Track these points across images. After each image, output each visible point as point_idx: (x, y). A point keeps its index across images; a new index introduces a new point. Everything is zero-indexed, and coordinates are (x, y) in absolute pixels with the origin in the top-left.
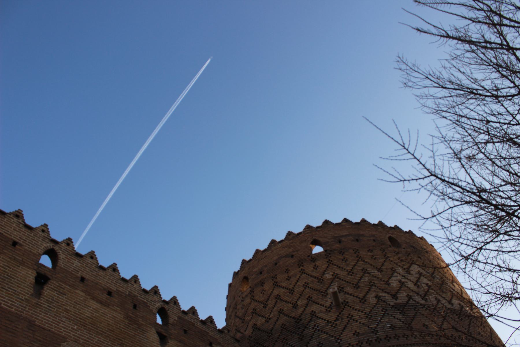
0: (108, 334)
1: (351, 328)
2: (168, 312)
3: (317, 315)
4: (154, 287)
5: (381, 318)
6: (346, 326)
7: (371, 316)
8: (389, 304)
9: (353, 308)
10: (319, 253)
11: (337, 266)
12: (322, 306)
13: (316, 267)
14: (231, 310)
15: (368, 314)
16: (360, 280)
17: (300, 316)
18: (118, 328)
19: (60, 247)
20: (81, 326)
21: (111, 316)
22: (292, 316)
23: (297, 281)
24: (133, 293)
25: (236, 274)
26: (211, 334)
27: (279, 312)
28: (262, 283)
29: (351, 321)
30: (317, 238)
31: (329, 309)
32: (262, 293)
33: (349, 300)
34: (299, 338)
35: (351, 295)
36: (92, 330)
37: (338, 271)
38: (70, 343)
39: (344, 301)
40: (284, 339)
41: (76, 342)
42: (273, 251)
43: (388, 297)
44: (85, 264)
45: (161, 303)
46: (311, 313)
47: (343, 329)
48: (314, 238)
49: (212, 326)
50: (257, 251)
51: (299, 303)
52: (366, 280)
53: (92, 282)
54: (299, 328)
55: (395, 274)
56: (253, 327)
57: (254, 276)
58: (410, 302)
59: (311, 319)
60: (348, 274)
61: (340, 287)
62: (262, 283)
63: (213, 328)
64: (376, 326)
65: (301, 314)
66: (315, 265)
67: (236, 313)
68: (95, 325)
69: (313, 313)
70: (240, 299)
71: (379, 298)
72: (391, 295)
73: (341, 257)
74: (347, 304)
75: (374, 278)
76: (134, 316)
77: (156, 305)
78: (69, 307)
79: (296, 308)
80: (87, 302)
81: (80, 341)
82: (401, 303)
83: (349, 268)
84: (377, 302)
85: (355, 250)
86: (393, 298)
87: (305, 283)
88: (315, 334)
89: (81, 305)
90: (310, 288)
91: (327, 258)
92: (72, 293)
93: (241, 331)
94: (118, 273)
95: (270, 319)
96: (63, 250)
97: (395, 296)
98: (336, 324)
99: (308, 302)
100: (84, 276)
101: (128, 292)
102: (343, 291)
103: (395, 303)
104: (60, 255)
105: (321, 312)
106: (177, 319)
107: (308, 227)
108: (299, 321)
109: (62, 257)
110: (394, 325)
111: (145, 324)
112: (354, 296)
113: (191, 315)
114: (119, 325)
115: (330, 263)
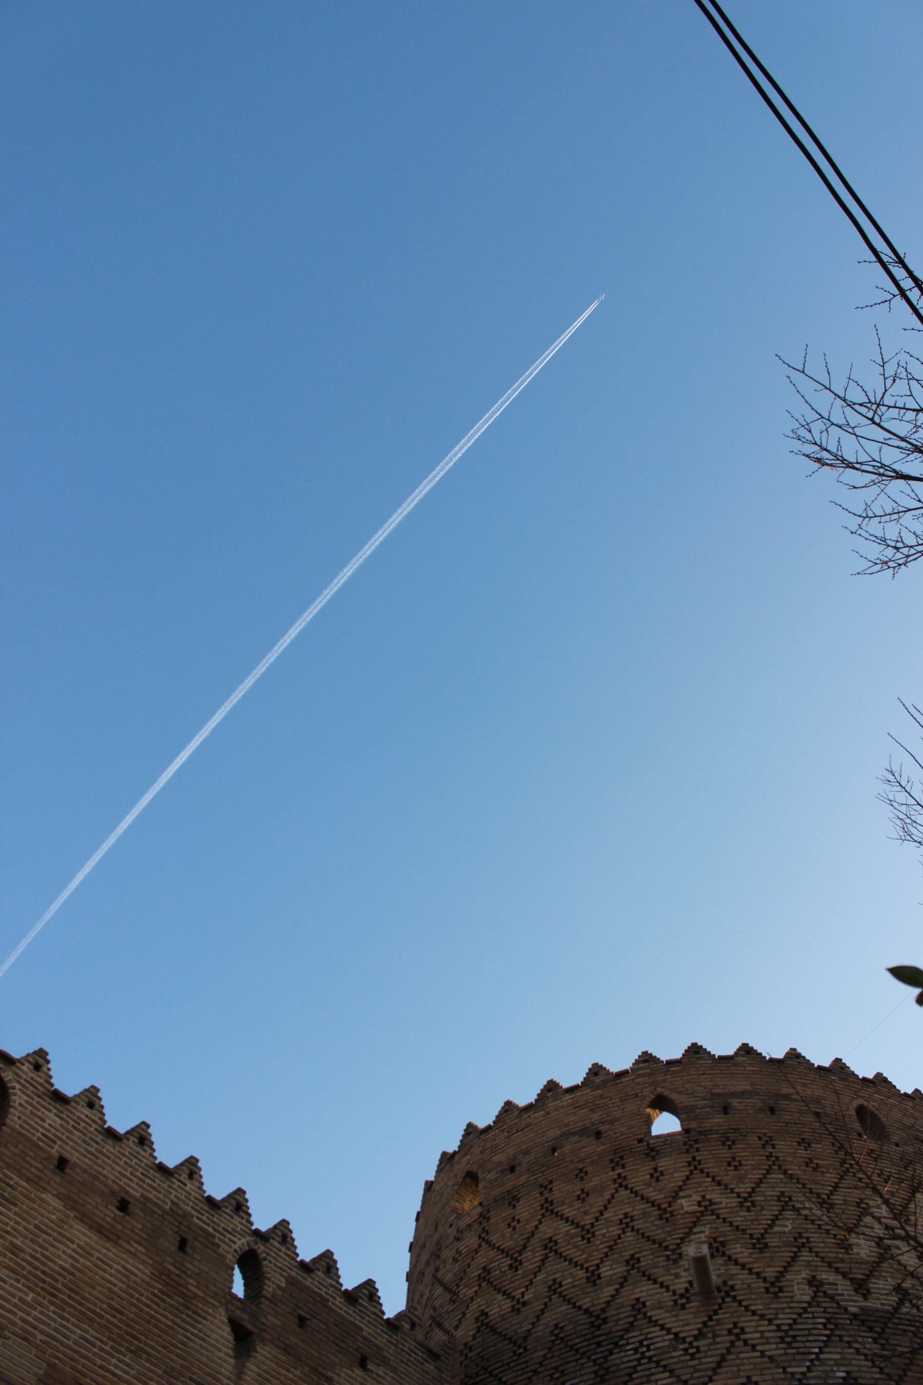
0: (108, 1321)
1: (738, 1366)
2: (265, 1263)
3: (649, 1314)
4: (235, 1192)
5: (820, 1348)
6: (723, 1358)
7: (794, 1337)
8: (846, 1310)
9: (746, 1307)
10: (668, 1135)
11: (713, 1178)
12: (664, 1290)
13: (656, 1175)
14: (425, 1257)
15: (786, 1331)
16: (771, 1226)
17: (603, 1310)
18: (134, 1305)
19: (17, 1074)
20: (43, 1293)
21: (120, 1268)
22: (584, 1307)
23: (606, 1208)
24: (182, 1205)
25: (446, 1159)
26: (367, 1331)
27: (550, 1287)
28: (514, 1198)
29: (737, 1343)
30: (666, 1093)
31: (681, 1301)
32: (509, 1225)
33: (738, 1284)
34: (595, 1372)
35: (743, 1266)
36: (71, 1306)
37: (714, 1194)
38: (10, 1342)
39: (725, 1283)
40: (556, 1368)
41: (25, 1339)
42: (549, 1113)
43: (843, 1287)
44: (72, 1123)
45: (248, 1238)
46: (633, 1306)
47: (714, 1365)
48: (659, 1090)
49: (373, 1309)
50: (509, 1106)
51: (605, 1270)
52: (786, 1229)
53: (85, 1171)
54: (599, 1344)
55: (868, 1220)
56: (477, 1319)
57: (492, 1175)
58: (905, 1310)
59: (631, 1323)
60: (741, 1205)
61: (715, 1239)
62: (513, 1199)
63: (374, 1313)
64: (804, 1369)
65: (608, 1303)
66: (656, 1169)
67: (437, 1270)
68: (77, 1293)
69: (639, 1306)
70: (452, 1232)
71: (817, 1286)
72: (851, 1280)
73: (725, 1153)
74: (732, 1293)
75: (810, 1226)
76: (178, 1272)
77: (235, 1243)
78: (21, 1238)
79: (594, 1284)
80: (66, 1227)
81: (35, 1337)
82: (877, 1310)
83: (744, 1188)
84: (813, 1298)
85: (765, 1138)
86: (856, 1290)
87: (626, 1215)
88: (639, 1368)
89: (50, 1235)
90: (638, 1230)
91: (688, 1152)
92: (34, 1202)
93: (447, 1325)
94: (149, 1151)
95: (524, 1304)
96: (22, 1081)
97: (861, 1287)
98: (697, 1348)
99: (628, 1271)
100: (67, 1155)
101: (169, 1202)
102: (724, 1254)
103: (861, 1308)
104: (15, 1094)
105: (660, 1305)
106: (283, 1285)
107: (647, 1059)
108: (599, 1322)
109: (18, 1101)
110: (854, 1375)
111: (202, 1295)
112: (750, 1270)
113: (320, 1274)
114: (137, 1295)
115: (696, 1168)
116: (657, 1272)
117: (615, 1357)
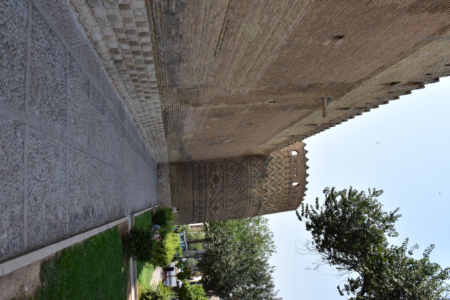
13: (286, 184)
51: (274, 177)
62: (289, 162)
116: (271, 184)
117: (261, 178)
